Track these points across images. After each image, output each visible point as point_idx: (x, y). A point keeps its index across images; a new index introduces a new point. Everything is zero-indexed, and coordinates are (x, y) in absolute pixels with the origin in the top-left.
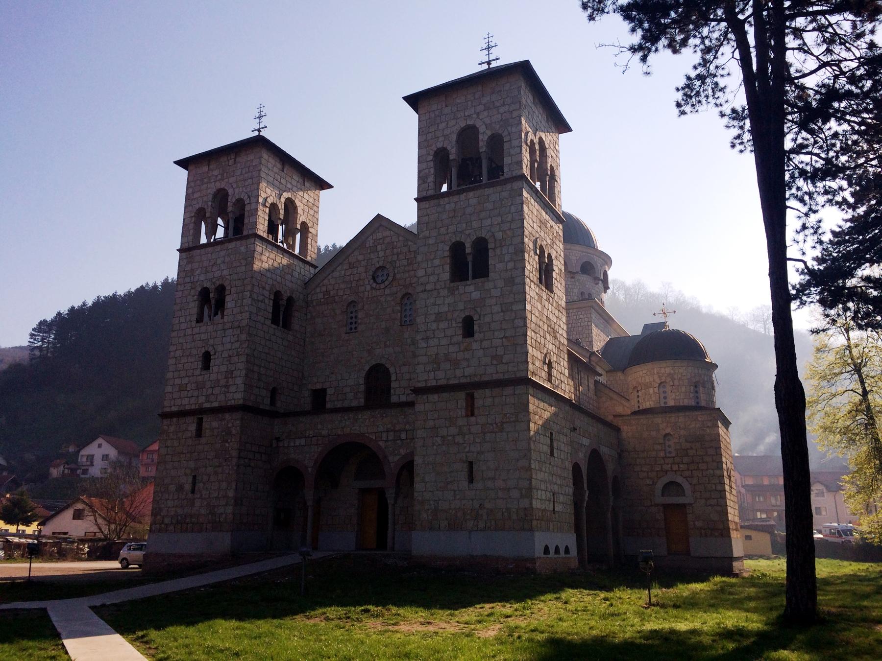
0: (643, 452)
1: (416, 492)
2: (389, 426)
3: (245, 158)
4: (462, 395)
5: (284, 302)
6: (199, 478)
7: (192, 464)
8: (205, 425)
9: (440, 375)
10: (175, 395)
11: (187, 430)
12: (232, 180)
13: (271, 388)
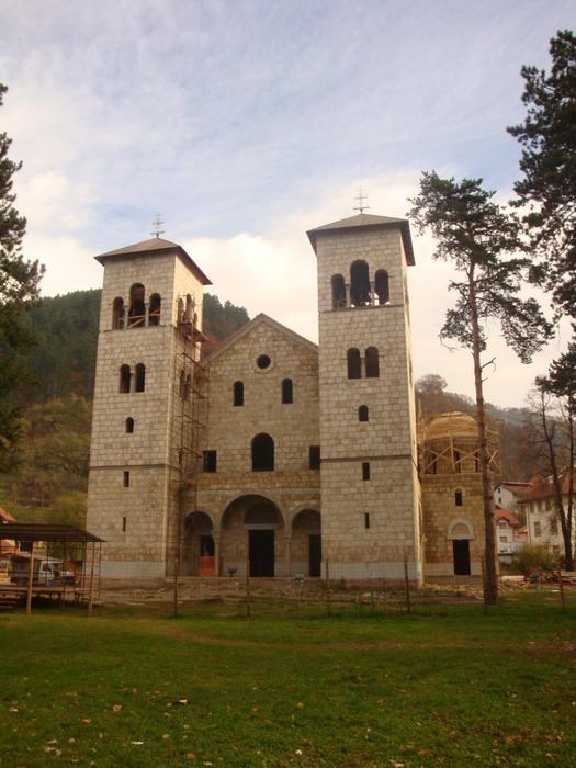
4: (359, 465)
7: (122, 508)
9: (341, 448)
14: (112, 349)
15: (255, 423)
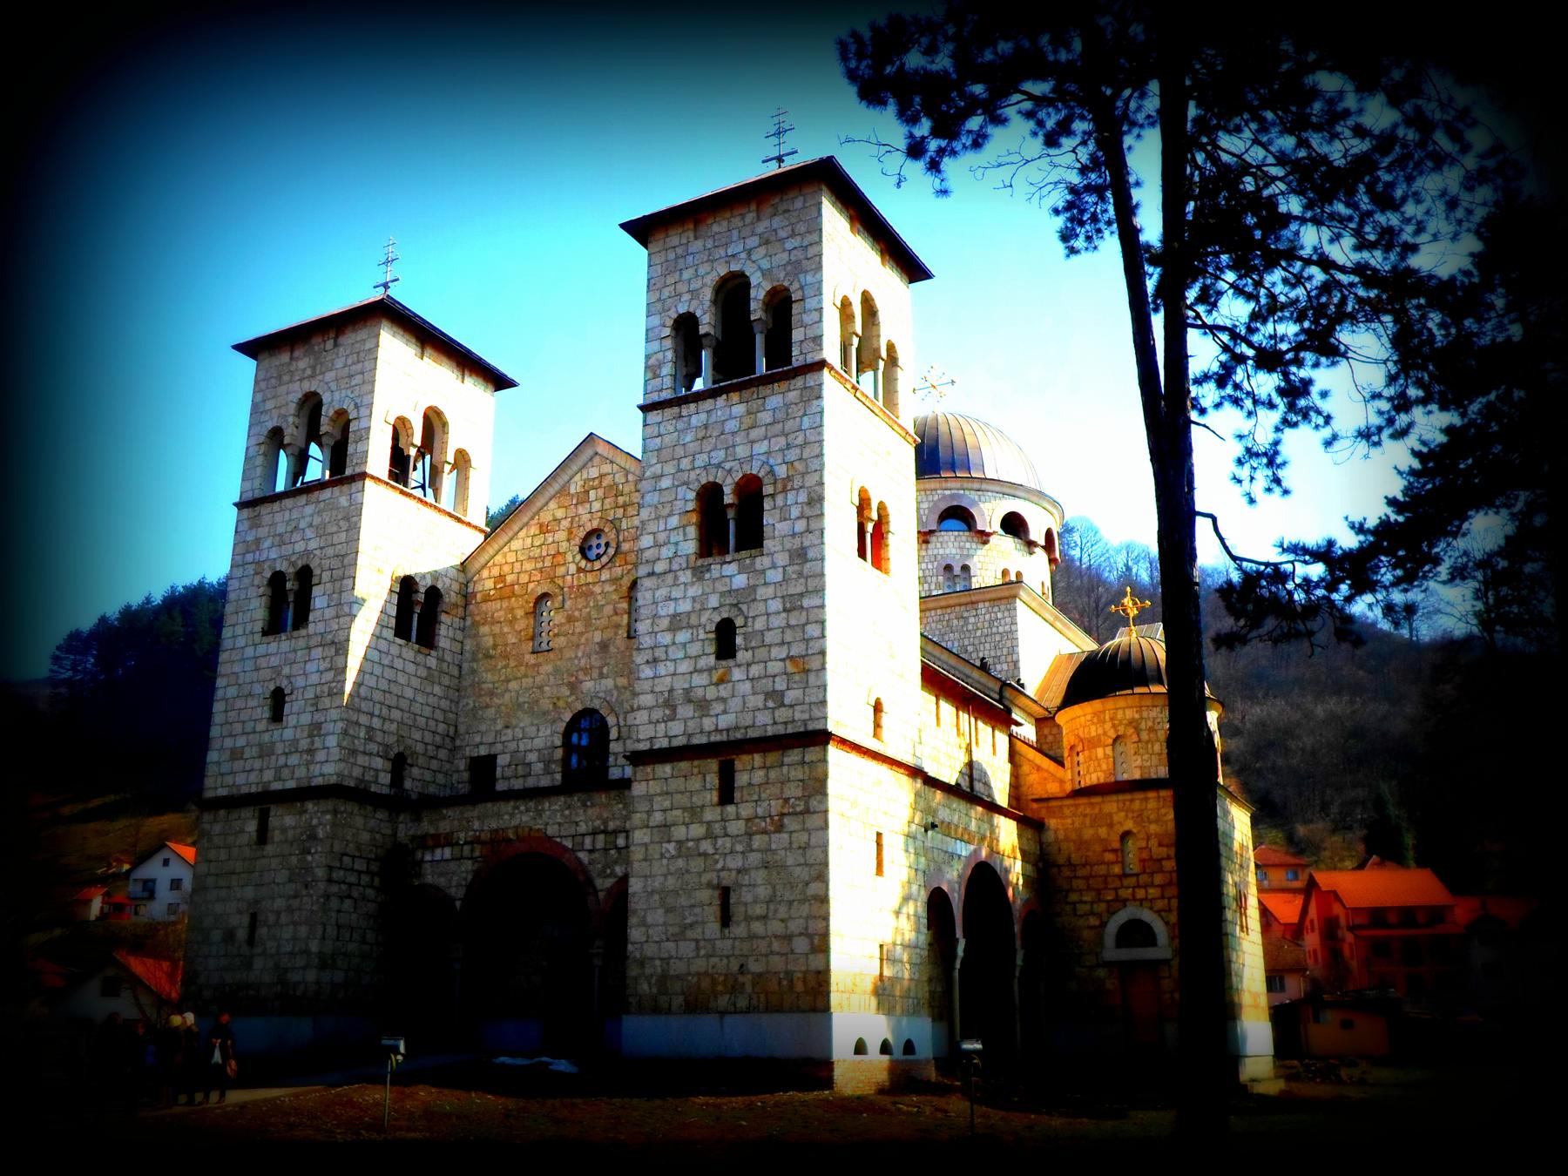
0: (1084, 866)
1: (633, 943)
2: (598, 823)
3: (350, 339)
4: (713, 765)
5: (421, 597)
6: (261, 917)
7: (250, 893)
8: (273, 821)
10: (225, 768)
11: (242, 831)
12: (330, 376)
13: (392, 755)
14: (258, 541)
15: (573, 687)
